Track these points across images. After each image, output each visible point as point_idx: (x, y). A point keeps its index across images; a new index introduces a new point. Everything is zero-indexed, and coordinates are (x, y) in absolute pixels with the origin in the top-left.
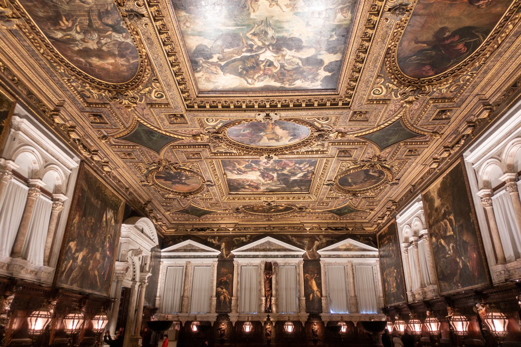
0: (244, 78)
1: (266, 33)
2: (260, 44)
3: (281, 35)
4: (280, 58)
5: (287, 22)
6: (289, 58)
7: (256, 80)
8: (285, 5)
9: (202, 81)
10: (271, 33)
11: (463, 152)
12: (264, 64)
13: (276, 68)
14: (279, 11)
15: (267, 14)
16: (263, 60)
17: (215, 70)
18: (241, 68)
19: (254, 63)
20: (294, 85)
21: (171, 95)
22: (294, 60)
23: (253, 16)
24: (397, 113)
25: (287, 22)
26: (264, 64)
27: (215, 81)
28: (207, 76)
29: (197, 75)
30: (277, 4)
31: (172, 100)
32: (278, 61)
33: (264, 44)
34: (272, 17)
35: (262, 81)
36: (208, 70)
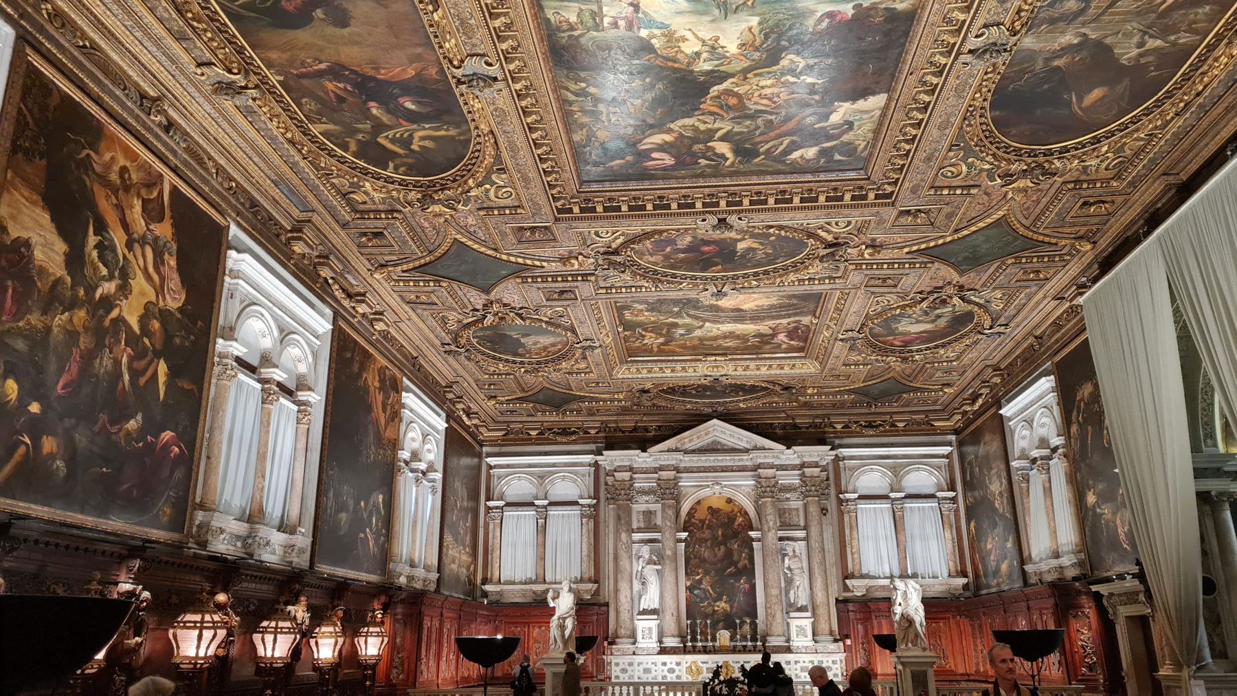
5: (680, 13)
8: (687, 40)
14: (699, 31)
23: (754, 21)
25: (680, 13)
30: (704, 42)
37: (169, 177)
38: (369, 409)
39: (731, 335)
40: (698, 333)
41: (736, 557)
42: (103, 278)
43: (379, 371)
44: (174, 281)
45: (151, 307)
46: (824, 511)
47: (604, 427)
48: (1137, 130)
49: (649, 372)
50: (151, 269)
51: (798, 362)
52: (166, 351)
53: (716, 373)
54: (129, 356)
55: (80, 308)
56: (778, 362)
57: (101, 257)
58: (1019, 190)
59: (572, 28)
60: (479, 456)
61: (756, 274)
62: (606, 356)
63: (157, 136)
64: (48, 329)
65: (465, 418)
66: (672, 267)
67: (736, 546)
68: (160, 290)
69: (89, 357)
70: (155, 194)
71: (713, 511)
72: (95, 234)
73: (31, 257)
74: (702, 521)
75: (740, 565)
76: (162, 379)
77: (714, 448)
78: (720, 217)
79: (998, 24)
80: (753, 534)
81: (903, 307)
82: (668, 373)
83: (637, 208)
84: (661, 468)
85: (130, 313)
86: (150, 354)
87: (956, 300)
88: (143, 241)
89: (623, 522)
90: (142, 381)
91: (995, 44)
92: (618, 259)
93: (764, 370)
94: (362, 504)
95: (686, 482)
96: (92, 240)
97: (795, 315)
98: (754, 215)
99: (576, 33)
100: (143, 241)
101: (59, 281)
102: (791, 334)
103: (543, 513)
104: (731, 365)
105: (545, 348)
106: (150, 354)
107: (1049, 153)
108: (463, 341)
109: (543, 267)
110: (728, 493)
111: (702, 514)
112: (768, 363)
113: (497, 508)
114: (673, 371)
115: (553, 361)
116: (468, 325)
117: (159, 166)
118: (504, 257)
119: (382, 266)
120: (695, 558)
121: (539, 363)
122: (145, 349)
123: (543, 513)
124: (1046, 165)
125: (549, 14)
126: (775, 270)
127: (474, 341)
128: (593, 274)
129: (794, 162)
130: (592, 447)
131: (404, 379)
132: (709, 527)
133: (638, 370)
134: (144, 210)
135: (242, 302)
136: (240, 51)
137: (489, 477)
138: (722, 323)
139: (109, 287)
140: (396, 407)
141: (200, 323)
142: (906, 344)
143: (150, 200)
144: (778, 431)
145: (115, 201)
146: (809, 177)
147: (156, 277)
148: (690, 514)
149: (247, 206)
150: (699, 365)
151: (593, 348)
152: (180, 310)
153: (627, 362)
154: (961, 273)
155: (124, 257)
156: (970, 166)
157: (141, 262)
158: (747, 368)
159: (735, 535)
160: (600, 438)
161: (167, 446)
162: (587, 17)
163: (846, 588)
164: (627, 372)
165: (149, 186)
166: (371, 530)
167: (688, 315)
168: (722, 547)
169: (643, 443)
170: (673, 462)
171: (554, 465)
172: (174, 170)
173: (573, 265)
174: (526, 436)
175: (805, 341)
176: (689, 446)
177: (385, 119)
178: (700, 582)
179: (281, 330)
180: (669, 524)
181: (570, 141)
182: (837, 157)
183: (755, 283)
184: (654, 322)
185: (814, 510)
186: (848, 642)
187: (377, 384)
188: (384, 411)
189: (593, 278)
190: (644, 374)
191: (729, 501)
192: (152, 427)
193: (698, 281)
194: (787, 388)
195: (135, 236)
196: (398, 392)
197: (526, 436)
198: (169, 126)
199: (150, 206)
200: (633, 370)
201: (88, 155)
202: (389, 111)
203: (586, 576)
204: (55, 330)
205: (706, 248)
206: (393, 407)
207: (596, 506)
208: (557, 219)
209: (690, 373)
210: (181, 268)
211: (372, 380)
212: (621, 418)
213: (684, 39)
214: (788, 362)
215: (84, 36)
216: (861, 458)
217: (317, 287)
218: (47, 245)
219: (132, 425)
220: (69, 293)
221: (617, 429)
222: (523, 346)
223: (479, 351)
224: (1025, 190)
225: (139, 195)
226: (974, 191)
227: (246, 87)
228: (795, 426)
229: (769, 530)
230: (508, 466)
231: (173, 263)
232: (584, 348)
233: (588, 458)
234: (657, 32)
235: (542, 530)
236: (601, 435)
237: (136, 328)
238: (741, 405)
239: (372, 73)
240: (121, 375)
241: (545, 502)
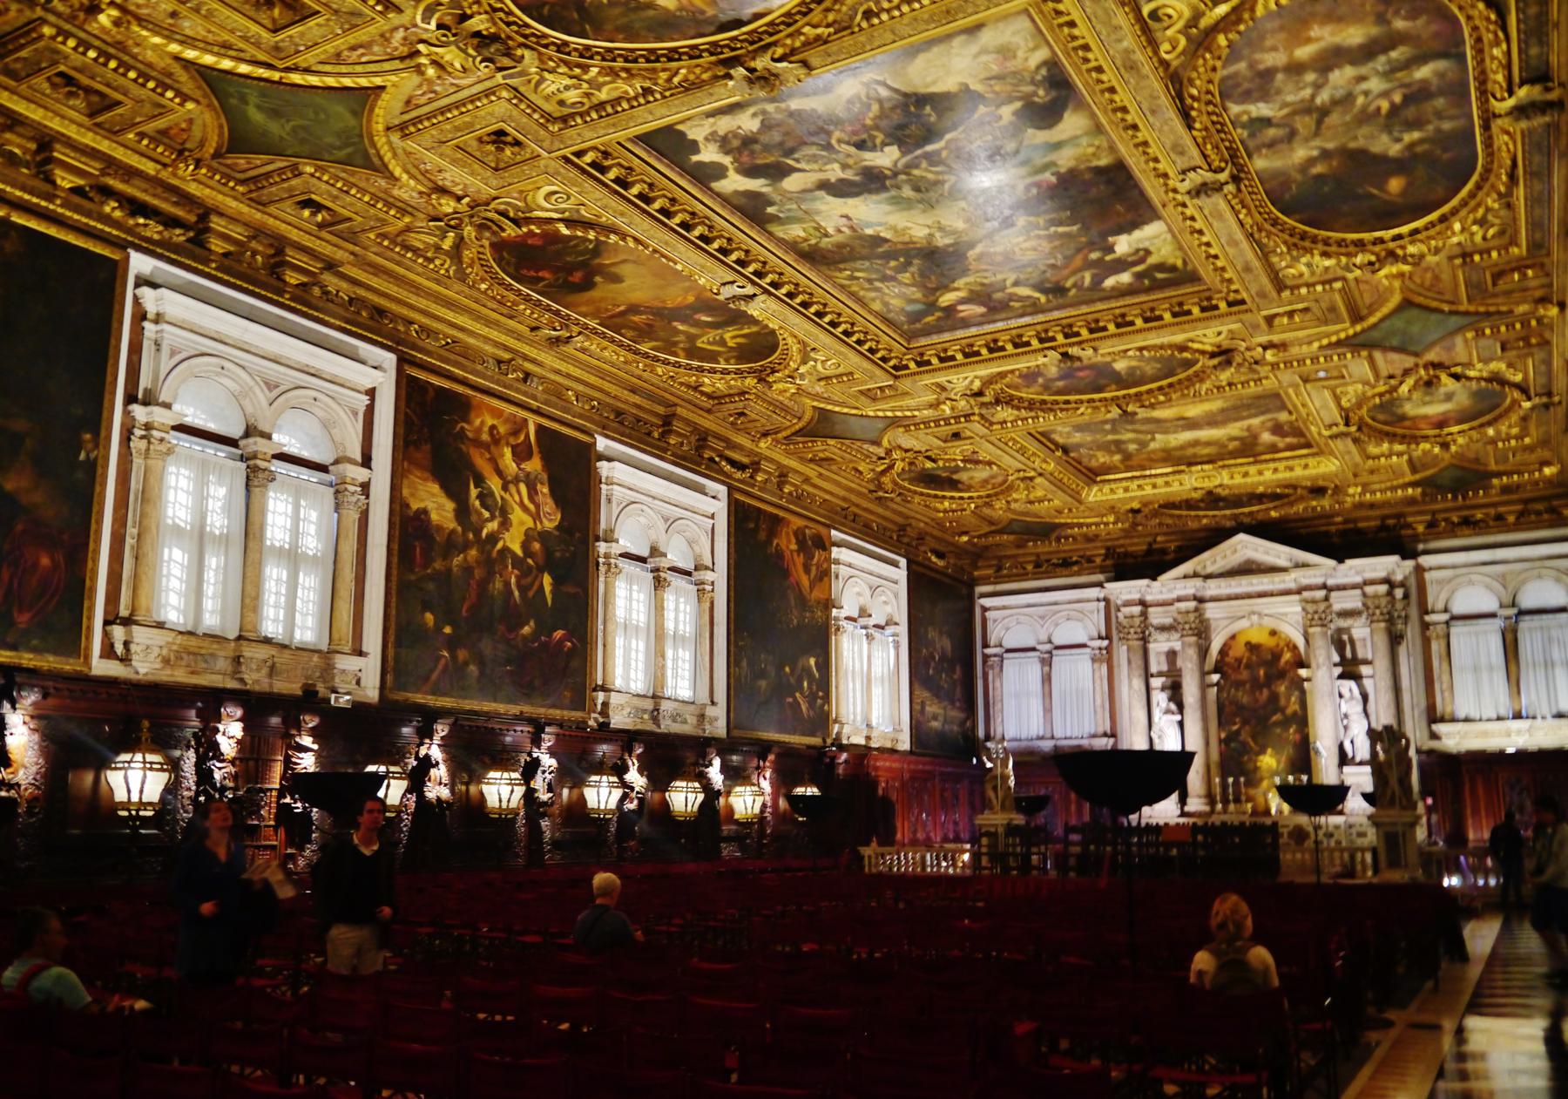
0: (906, 95)
1: (917, 189)
2: (916, 172)
3: (884, 195)
4: (851, 161)
6: (828, 167)
7: (868, 97)
9: (1022, 44)
10: (907, 192)
11: (139, 249)
12: (878, 141)
13: (839, 141)
15: (935, 212)
16: (887, 149)
17: (997, 88)
18: (930, 115)
19: (905, 136)
20: (754, 115)
21: (1120, 41)
22: (815, 167)
24: (413, 171)
26: (878, 141)
27: (984, 58)
28: (1014, 62)
29: (1042, 54)
31: (1114, 22)
32: (849, 156)
33: (908, 174)
34: (924, 211)
35: (850, 101)
36: (1015, 81)
37: (533, 421)
38: (786, 573)
39: (1196, 443)
40: (1153, 446)
41: (1283, 702)
42: (488, 520)
43: (796, 533)
44: (548, 505)
45: (531, 533)
46: (1395, 639)
47: (1110, 552)
48: (1479, 205)
49: (1126, 490)
50: (526, 501)
51: (1311, 461)
52: (549, 564)
53: (1208, 484)
54: (517, 577)
55: (471, 548)
56: (1284, 463)
57: (483, 505)
58: (1394, 276)
59: (806, 240)
60: (971, 599)
61: (1160, 388)
62: (1058, 484)
63: (518, 391)
64: (449, 570)
65: (934, 559)
66: (1059, 393)
67: (1283, 688)
68: (536, 517)
69: (484, 584)
70: (522, 437)
71: (1252, 647)
72: (476, 487)
73: (429, 520)
74: (1239, 660)
75: (1289, 711)
76: (548, 588)
77: (1248, 569)
78: (1061, 350)
79: (1194, 169)
80: (1303, 672)
81: (1381, 395)
82: (1149, 491)
83: (970, 353)
84: (1179, 600)
85: (512, 541)
86: (534, 571)
87: (1444, 378)
88: (516, 480)
89: (1134, 665)
90: (531, 594)
91: (1204, 184)
92: (986, 399)
93: (1268, 475)
94: (787, 669)
95: (1212, 611)
96: (474, 492)
97: (1263, 413)
98: (1096, 344)
99: (813, 242)
100: (516, 480)
101: (453, 531)
102: (1277, 429)
103: (1047, 662)
104: (1225, 473)
105: (986, 481)
106: (534, 571)
107: (1399, 237)
108: (890, 486)
109: (914, 416)
110: (1269, 623)
111: (1238, 650)
112: (1272, 465)
113: (995, 655)
114: (1154, 486)
115: (1002, 492)
116: (883, 472)
117: (523, 414)
118: (871, 414)
119: (765, 435)
120: (1231, 703)
121: (988, 496)
122: (530, 567)
123: (1047, 662)
124: (1400, 252)
125: (781, 235)
126: (1180, 382)
127: (906, 484)
128: (974, 414)
129: (1113, 288)
130: (1100, 577)
131: (833, 532)
132: (1248, 666)
133: (1112, 490)
134: (514, 454)
135: (618, 505)
136: (557, 313)
137: (984, 621)
138: (1175, 432)
139: (493, 526)
140: (825, 566)
141: (577, 535)
142: (1441, 423)
143: (518, 445)
144: (1336, 540)
145: (488, 456)
146: (1143, 298)
147: (531, 507)
148: (1223, 652)
149: (612, 417)
150: (1185, 477)
151: (1031, 479)
152: (558, 528)
153: (1095, 482)
154: (1416, 354)
155: (502, 498)
156: (1309, 265)
157: (517, 498)
158: (1246, 475)
159: (1282, 675)
160: (1107, 566)
161: (562, 640)
162: (812, 231)
163: (1434, 736)
164: (1099, 494)
165: (515, 433)
166: (802, 694)
167: (1128, 431)
168: (1266, 692)
169: (1151, 565)
170: (1191, 591)
171: (1056, 604)
172: (537, 412)
173: (944, 411)
174: (1022, 571)
175: (1302, 434)
176: (1210, 569)
177: (693, 330)
178: (1238, 733)
179: (666, 520)
180: (1189, 665)
181: (870, 311)
182: (1160, 276)
183: (1162, 398)
184: (1093, 442)
185: (1382, 641)
186: (1430, 801)
187: (794, 547)
188: (807, 570)
189: (976, 418)
190: (1120, 494)
191: (1273, 633)
192: (544, 628)
193: (1098, 404)
194: (1318, 491)
195: (509, 478)
196: (824, 548)
197: (1022, 571)
199: (519, 449)
200: (1106, 488)
201: (462, 428)
202: (692, 326)
203: (1100, 730)
204: (455, 569)
205: (1081, 374)
206: (818, 566)
207: (1109, 649)
208: (896, 377)
209: (1175, 487)
211: (787, 543)
212: (1128, 541)
213: (910, 228)
214: (1297, 462)
215: (446, 336)
216: (1454, 567)
217: (702, 469)
218: (440, 507)
219: (526, 630)
220: (460, 539)
221: (1126, 554)
222: (958, 482)
223: (915, 492)
224: (1401, 275)
225: (508, 444)
226: (1338, 285)
227: (571, 337)
228: (1358, 531)
229: (1318, 667)
230: (1004, 608)
231: (546, 490)
232: (1023, 479)
233: (1094, 592)
234: (879, 228)
235: (1047, 679)
236: (1109, 562)
237: (519, 552)
238: (1273, 514)
239: (660, 305)
240: (511, 593)
241: (1048, 647)
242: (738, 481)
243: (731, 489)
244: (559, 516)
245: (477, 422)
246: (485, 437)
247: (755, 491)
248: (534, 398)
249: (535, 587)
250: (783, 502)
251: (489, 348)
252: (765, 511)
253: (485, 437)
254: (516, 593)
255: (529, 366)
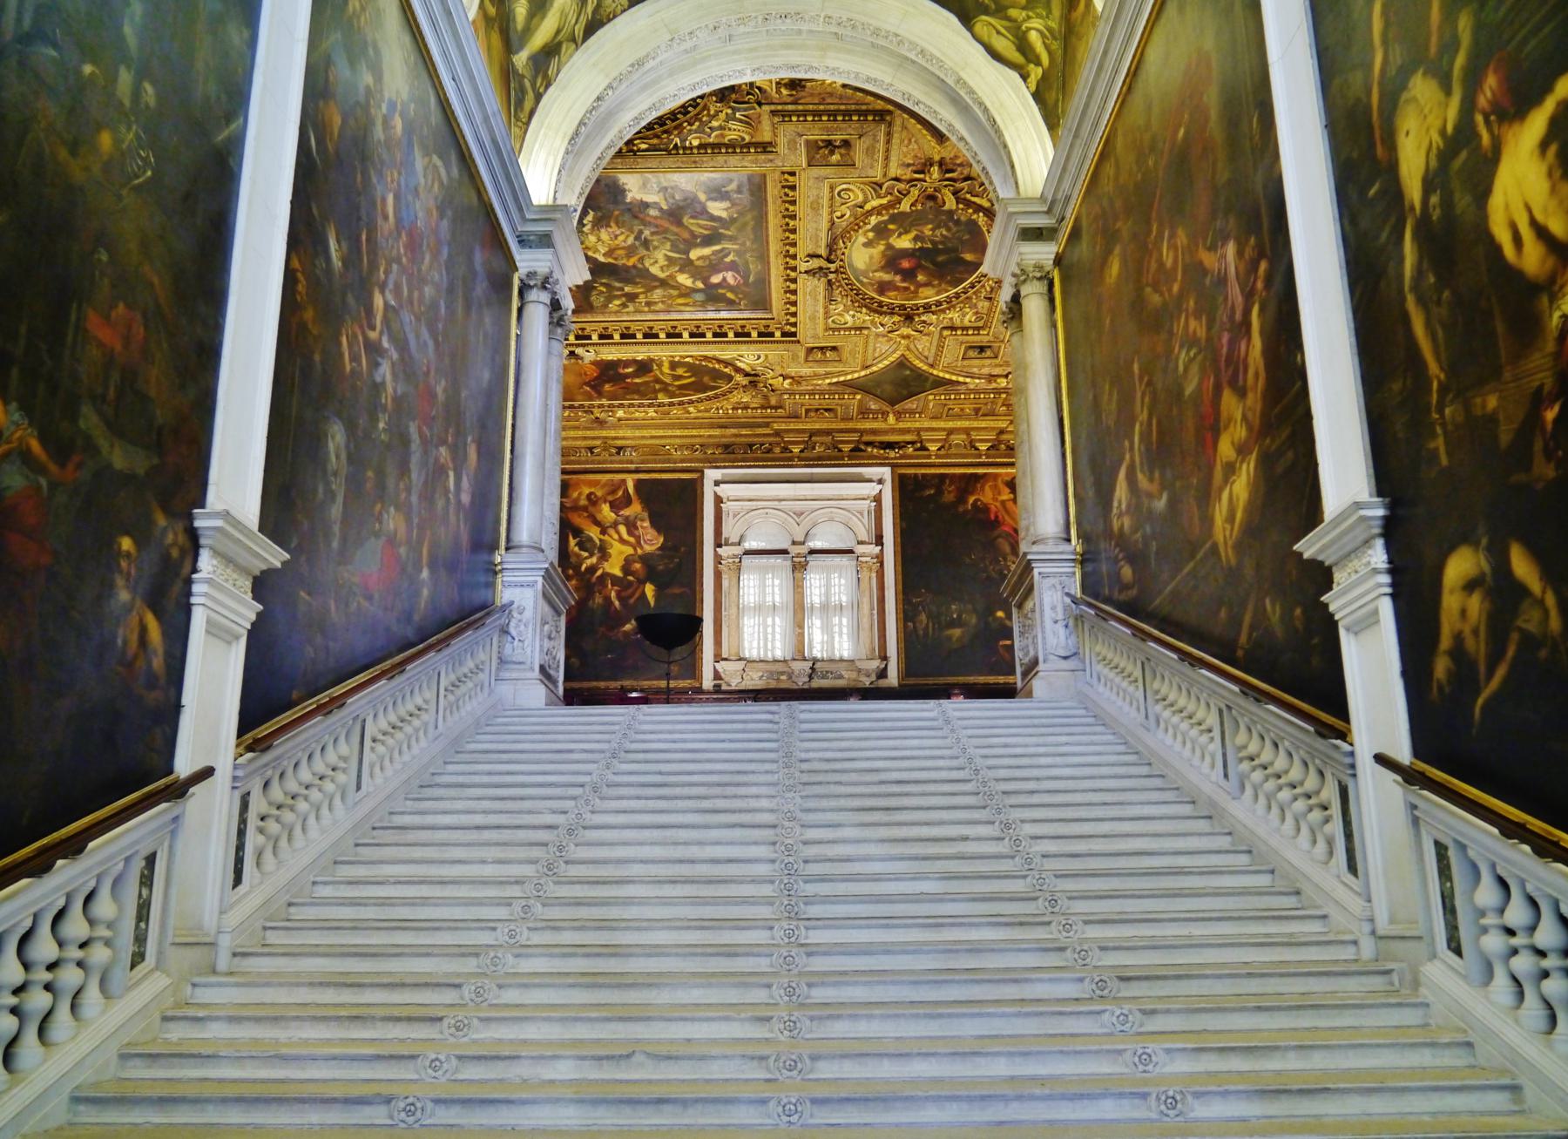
50: (625, 536)
52: (651, 575)
63: (612, 462)
70: (620, 493)
85: (612, 567)
86: (635, 585)
88: (615, 525)
90: (632, 601)
100: (615, 525)
106: (635, 585)
122: (630, 583)
147: (632, 540)
152: (659, 549)
155: (601, 540)
157: (616, 536)
165: (613, 492)
198: (620, 449)
210: (654, 524)
219: (628, 627)
225: (605, 502)
231: (646, 524)
240: (612, 603)
242: (895, 458)
243: (893, 466)
244: (661, 540)
245: (575, 495)
246: (583, 502)
247: (933, 460)
248: (632, 463)
249: (637, 595)
250: (984, 459)
251: (579, 443)
252: (954, 475)
253: (583, 502)
254: (617, 603)
255: (619, 443)
